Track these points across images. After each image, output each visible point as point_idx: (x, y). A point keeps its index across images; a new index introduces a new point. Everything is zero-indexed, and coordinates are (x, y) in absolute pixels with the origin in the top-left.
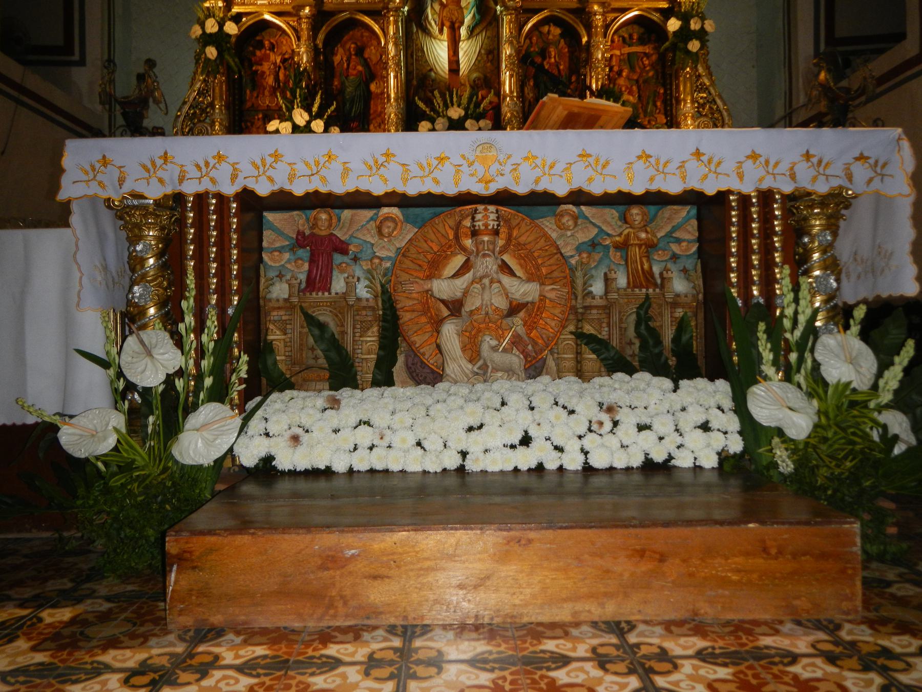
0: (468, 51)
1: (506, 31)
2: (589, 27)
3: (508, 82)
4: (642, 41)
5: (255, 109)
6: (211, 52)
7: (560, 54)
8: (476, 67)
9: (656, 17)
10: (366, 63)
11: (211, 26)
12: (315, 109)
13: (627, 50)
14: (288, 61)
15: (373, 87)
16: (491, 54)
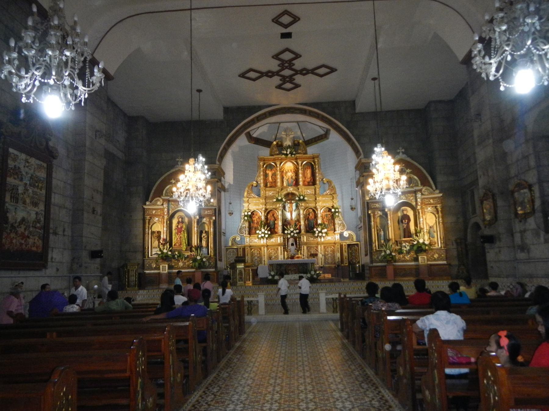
0: (294, 214)
1: (301, 212)
2: (317, 210)
3: (302, 223)
4: (329, 211)
5: (253, 227)
6: (246, 218)
7: (312, 214)
8: (296, 217)
9: (331, 208)
10: (274, 218)
11: (246, 214)
12: (266, 228)
13: (325, 213)
14: (260, 218)
15: (276, 222)
16: (299, 215)
